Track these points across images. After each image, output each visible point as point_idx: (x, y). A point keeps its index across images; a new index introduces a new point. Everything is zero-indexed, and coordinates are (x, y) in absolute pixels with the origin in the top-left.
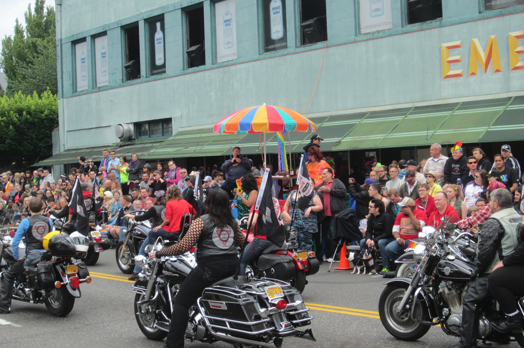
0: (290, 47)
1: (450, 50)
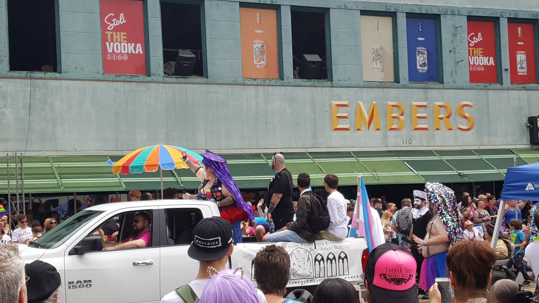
0: (155, 75)
1: (339, 108)
